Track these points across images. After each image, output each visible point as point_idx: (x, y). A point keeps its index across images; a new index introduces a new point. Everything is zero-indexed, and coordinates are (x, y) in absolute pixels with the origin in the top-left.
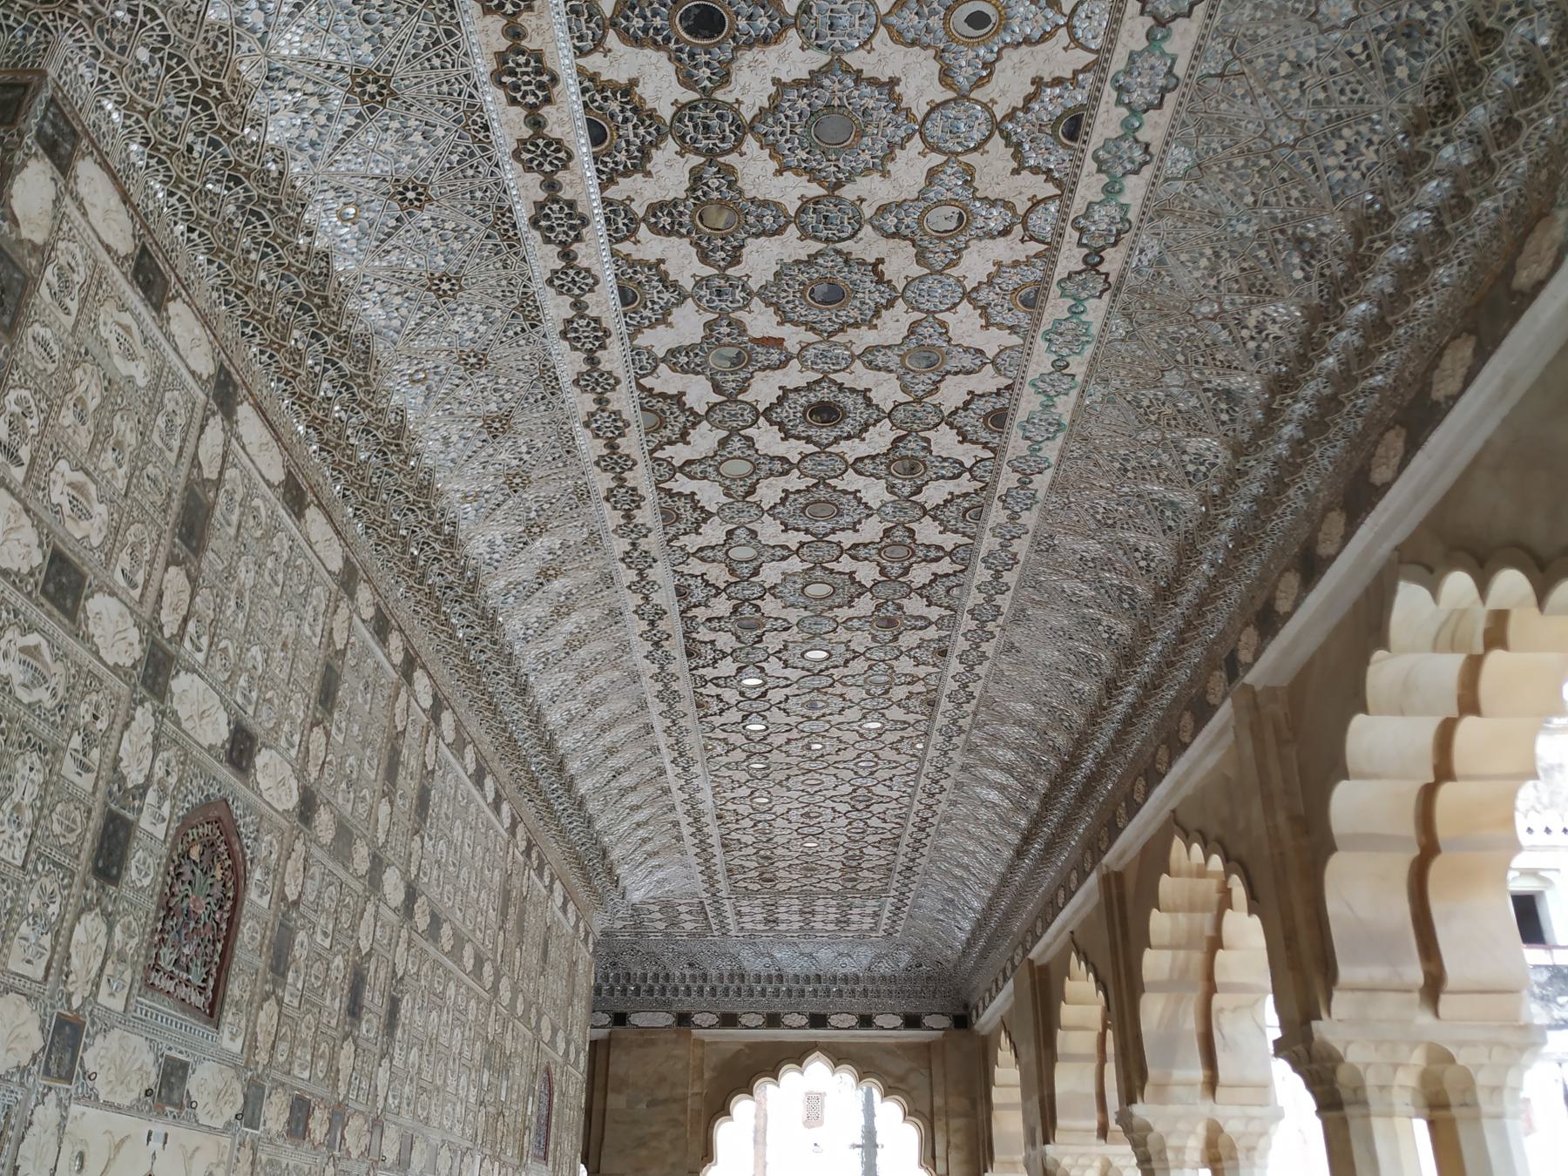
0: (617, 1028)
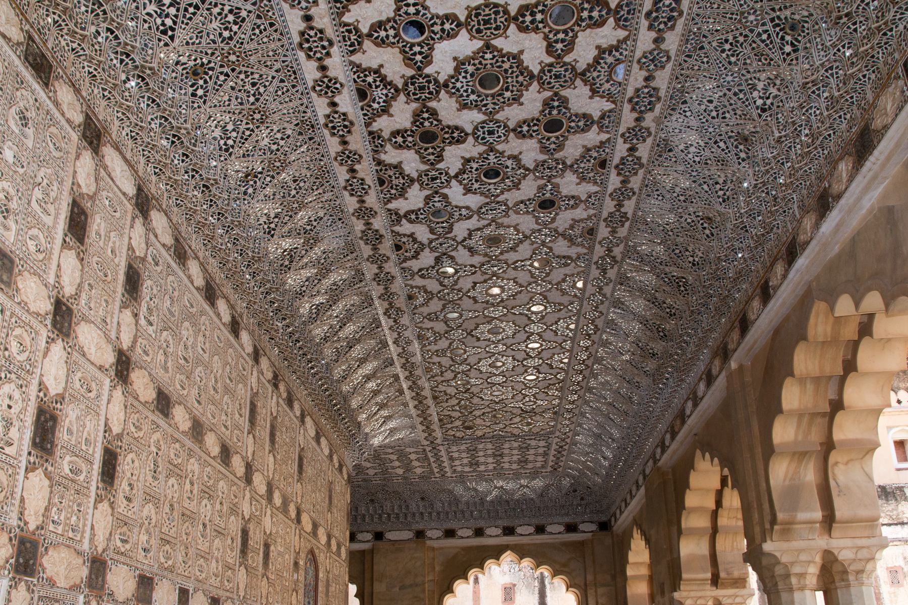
0: (379, 543)
